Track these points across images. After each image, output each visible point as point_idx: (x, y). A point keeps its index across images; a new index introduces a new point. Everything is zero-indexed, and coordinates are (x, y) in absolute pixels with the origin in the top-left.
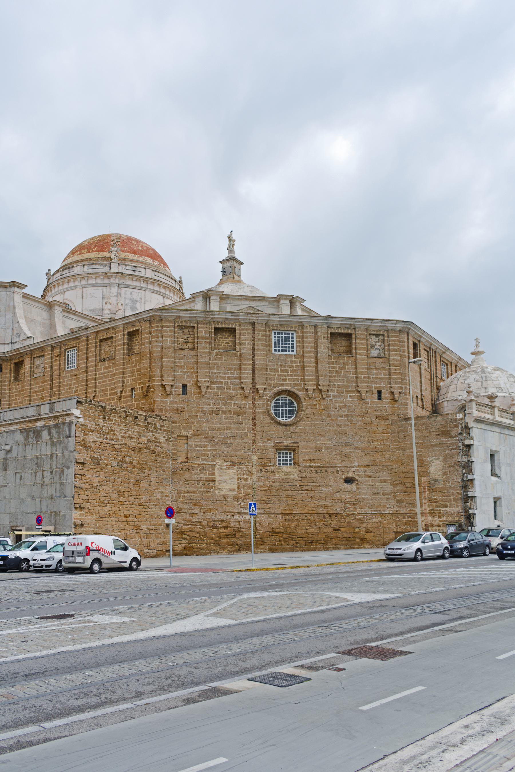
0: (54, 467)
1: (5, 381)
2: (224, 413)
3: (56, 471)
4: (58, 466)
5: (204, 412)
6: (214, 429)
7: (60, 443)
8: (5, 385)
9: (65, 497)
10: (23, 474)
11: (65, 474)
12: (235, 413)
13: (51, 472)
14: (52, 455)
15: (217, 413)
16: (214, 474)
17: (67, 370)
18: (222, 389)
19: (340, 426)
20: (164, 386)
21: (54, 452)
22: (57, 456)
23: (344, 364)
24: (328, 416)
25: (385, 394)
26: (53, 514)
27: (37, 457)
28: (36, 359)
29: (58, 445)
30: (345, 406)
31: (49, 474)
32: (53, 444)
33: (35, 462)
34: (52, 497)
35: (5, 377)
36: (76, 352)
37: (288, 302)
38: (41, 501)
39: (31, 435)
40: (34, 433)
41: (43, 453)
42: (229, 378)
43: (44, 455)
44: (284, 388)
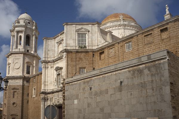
0: (155, 86)
1: (96, 60)
3: (156, 89)
4: (158, 86)
7: (158, 74)
8: (96, 62)
9: (165, 101)
10: (132, 92)
11: (163, 89)
13: (153, 90)
14: (152, 81)
17: (126, 51)
21: (154, 79)
22: (156, 81)
26: (157, 111)
27: (141, 83)
28: (110, 50)
29: (156, 75)
31: (151, 90)
32: (152, 75)
33: (141, 86)
34: (155, 102)
35: (96, 59)
36: (131, 43)
38: (147, 104)
39: (136, 72)
40: (138, 71)
41: (146, 80)
43: (146, 81)
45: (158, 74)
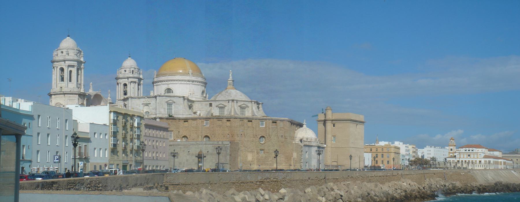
2: (250, 141)
5: (245, 141)
6: (247, 145)
12: (252, 141)
15: (248, 141)
16: (247, 156)
18: (249, 135)
19: (273, 144)
20: (237, 135)
23: (275, 129)
24: (271, 142)
25: (283, 136)
30: (275, 140)
37: (254, 102)
42: (251, 133)
44: (262, 135)
45: (225, 150)
